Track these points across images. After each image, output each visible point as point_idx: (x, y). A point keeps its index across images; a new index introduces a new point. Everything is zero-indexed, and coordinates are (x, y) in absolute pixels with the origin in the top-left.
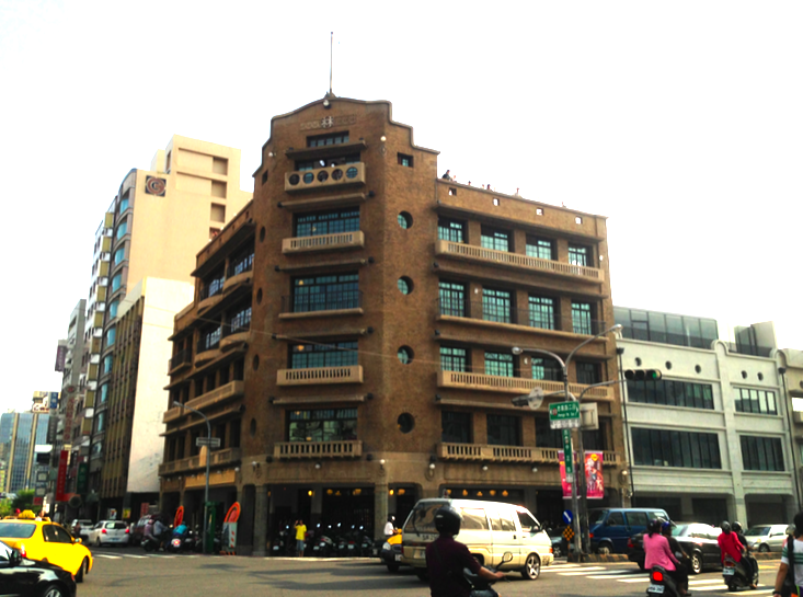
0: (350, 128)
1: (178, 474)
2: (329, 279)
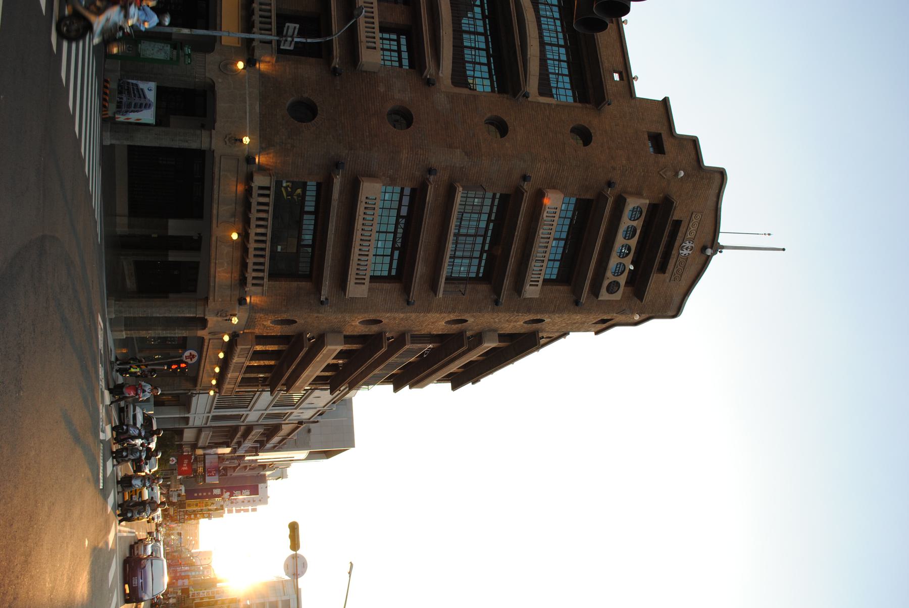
0: (668, 275)
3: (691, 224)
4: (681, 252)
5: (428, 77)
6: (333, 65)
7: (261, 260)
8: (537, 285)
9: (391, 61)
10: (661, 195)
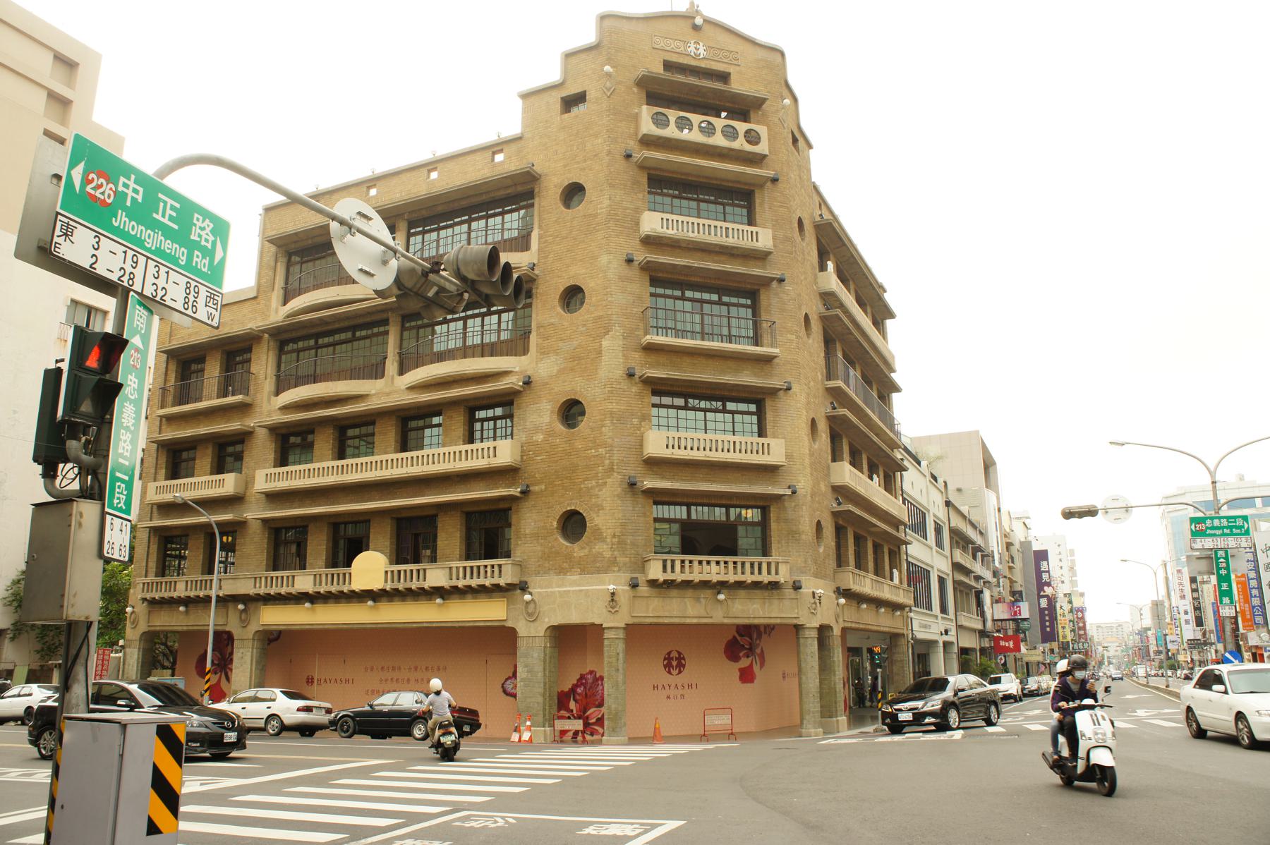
0: (731, 69)
1: (235, 599)
2: (706, 296)
3: (668, 48)
5: (521, 384)
6: (518, 495)
7: (748, 566)
8: (757, 233)
9: (506, 427)
10: (635, 90)
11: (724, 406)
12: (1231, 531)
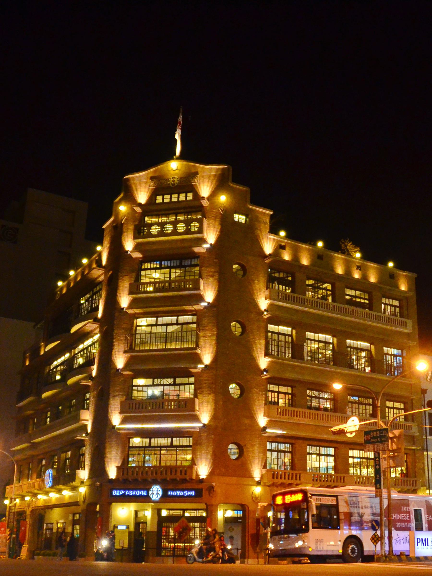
4: (176, 184)
11: (174, 381)
12: (381, 439)
